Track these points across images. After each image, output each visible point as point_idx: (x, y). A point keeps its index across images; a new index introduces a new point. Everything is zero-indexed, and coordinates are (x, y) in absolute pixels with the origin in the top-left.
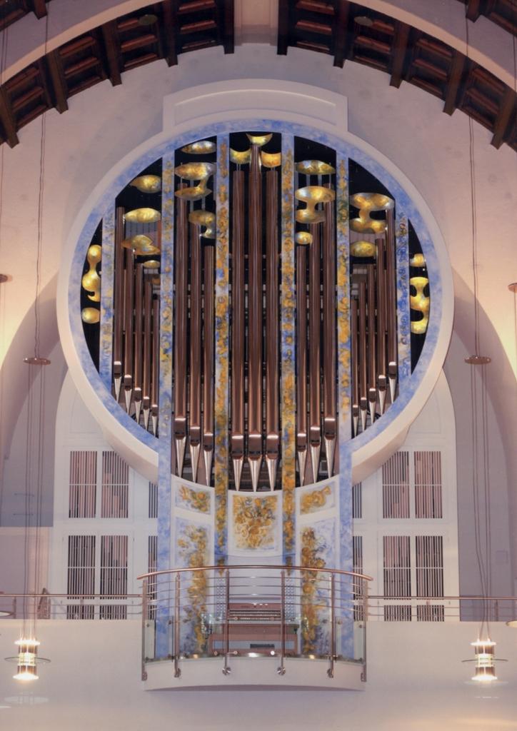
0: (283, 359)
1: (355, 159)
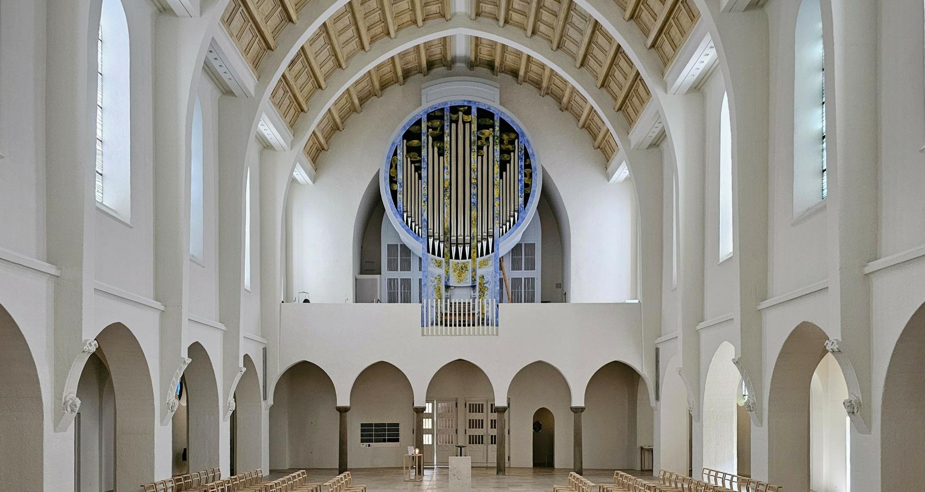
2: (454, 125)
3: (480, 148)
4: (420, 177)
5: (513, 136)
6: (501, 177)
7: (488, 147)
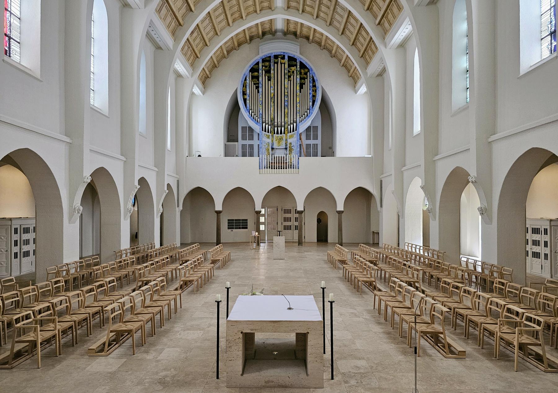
2: (276, 65)
3: (289, 77)
4: (258, 92)
5: (306, 70)
6: (300, 92)
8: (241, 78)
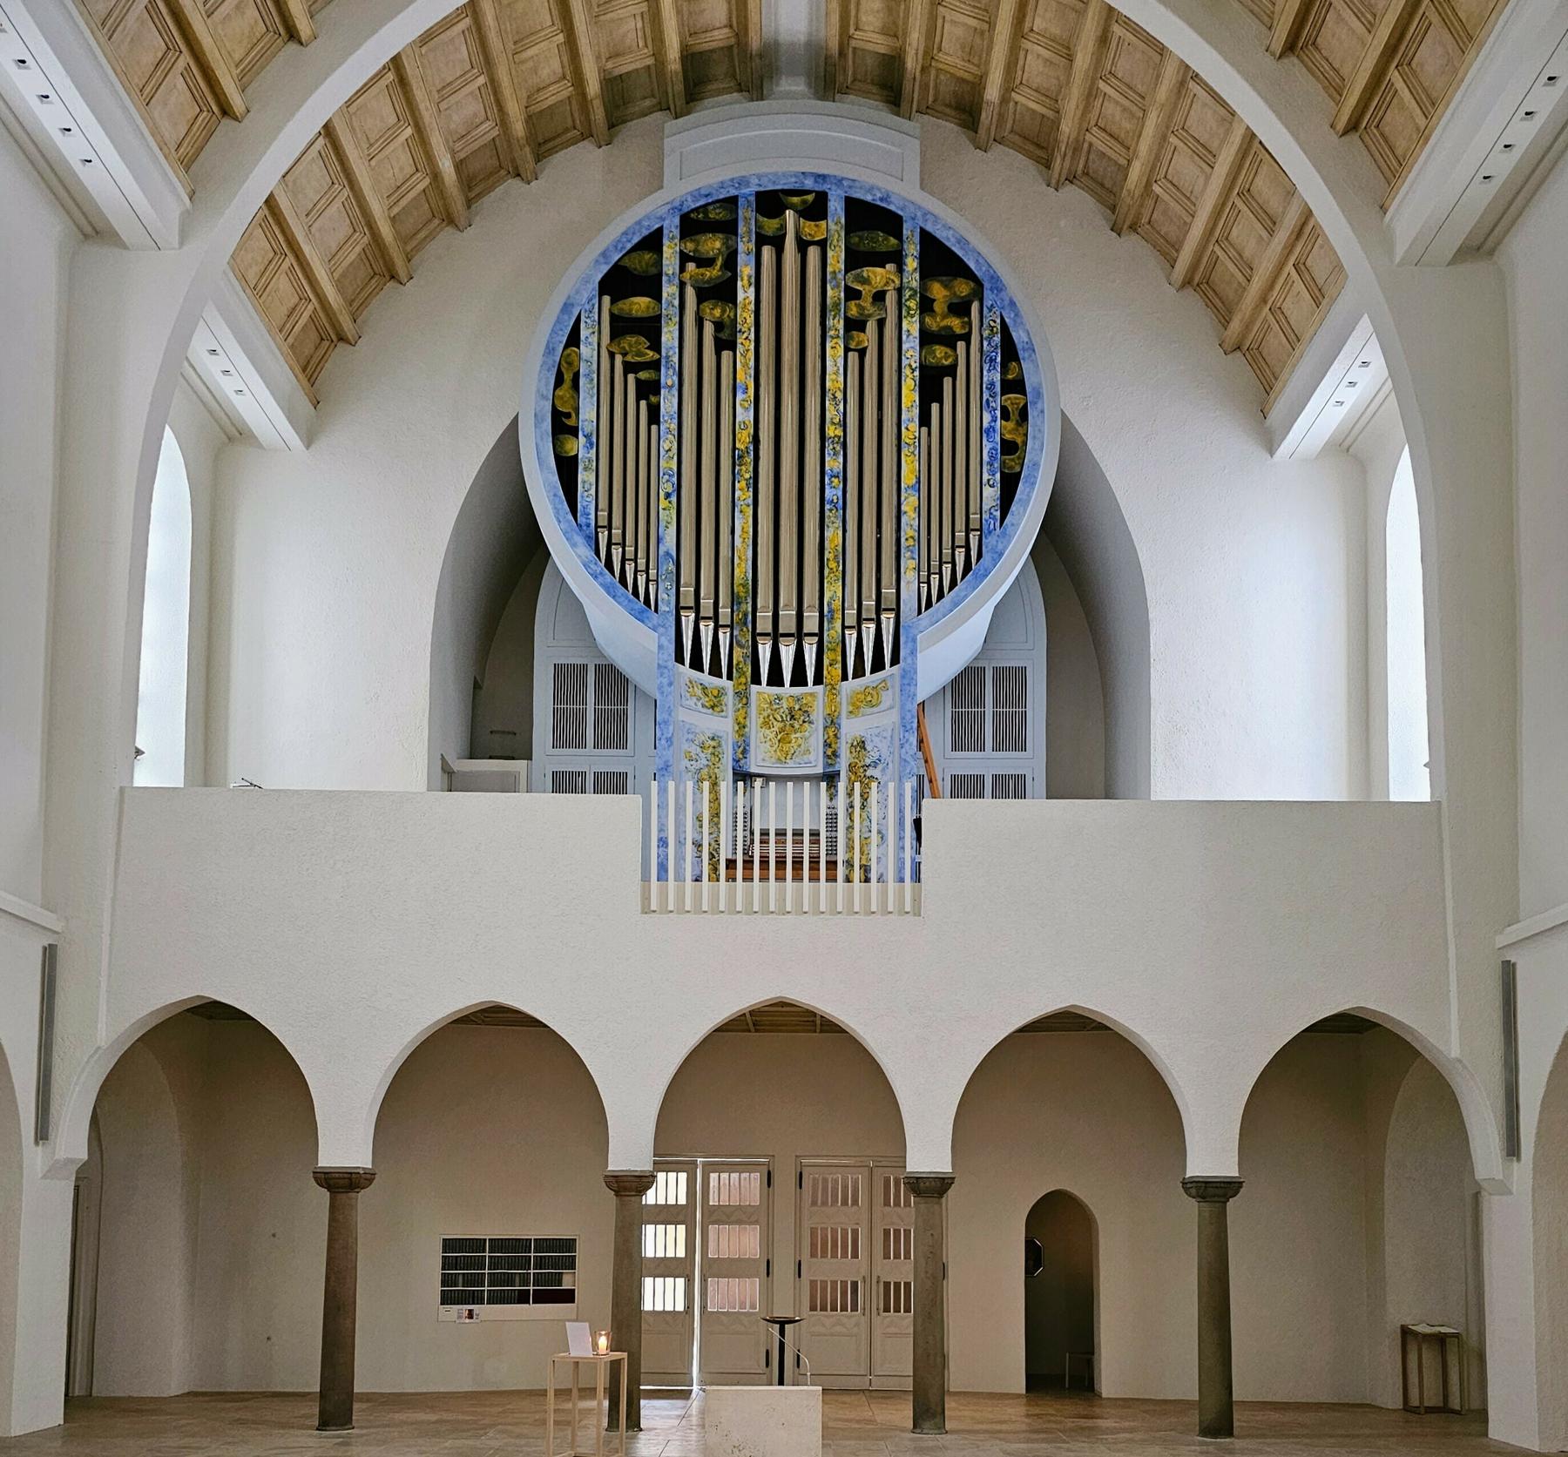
0: (827, 507)
1: (929, 228)
2: (767, 252)
3: (854, 325)
4: (654, 416)
5: (963, 288)
6: (925, 420)
7: (881, 323)
8: (544, 331)
